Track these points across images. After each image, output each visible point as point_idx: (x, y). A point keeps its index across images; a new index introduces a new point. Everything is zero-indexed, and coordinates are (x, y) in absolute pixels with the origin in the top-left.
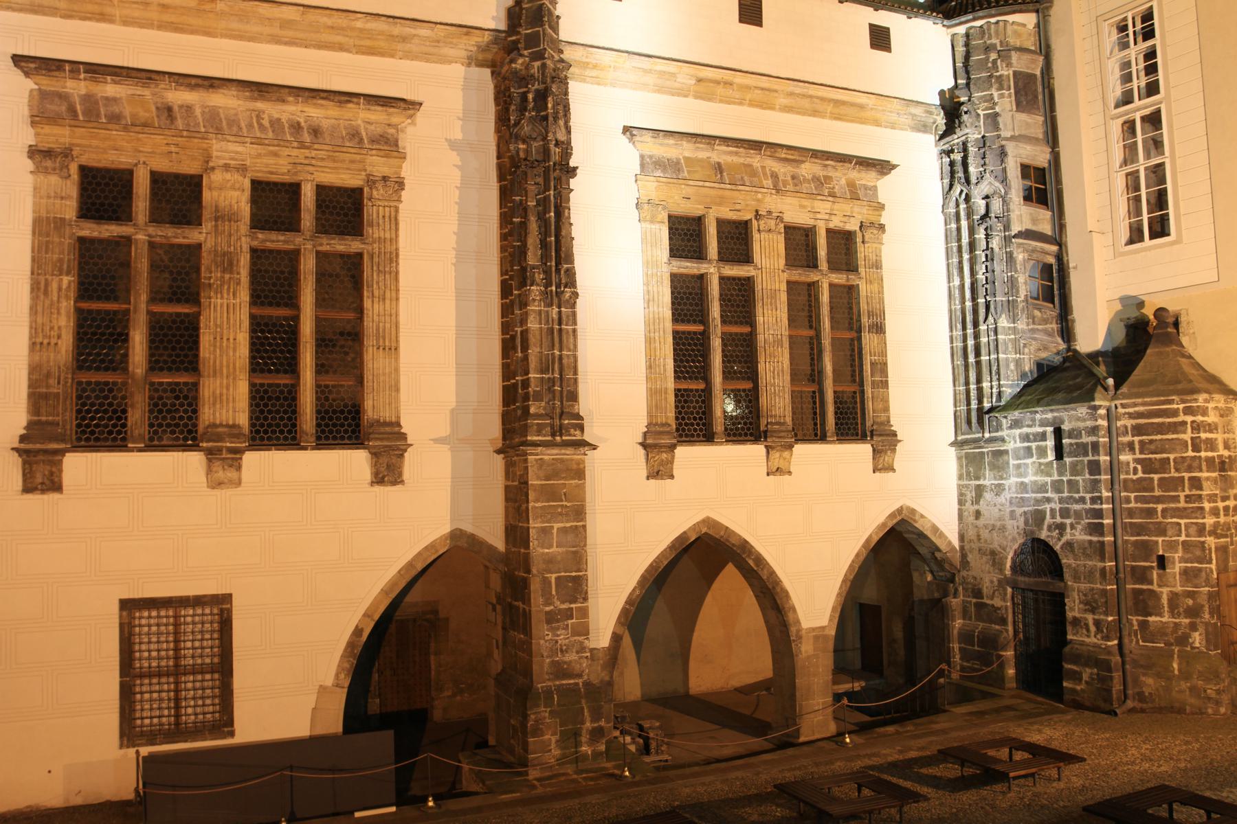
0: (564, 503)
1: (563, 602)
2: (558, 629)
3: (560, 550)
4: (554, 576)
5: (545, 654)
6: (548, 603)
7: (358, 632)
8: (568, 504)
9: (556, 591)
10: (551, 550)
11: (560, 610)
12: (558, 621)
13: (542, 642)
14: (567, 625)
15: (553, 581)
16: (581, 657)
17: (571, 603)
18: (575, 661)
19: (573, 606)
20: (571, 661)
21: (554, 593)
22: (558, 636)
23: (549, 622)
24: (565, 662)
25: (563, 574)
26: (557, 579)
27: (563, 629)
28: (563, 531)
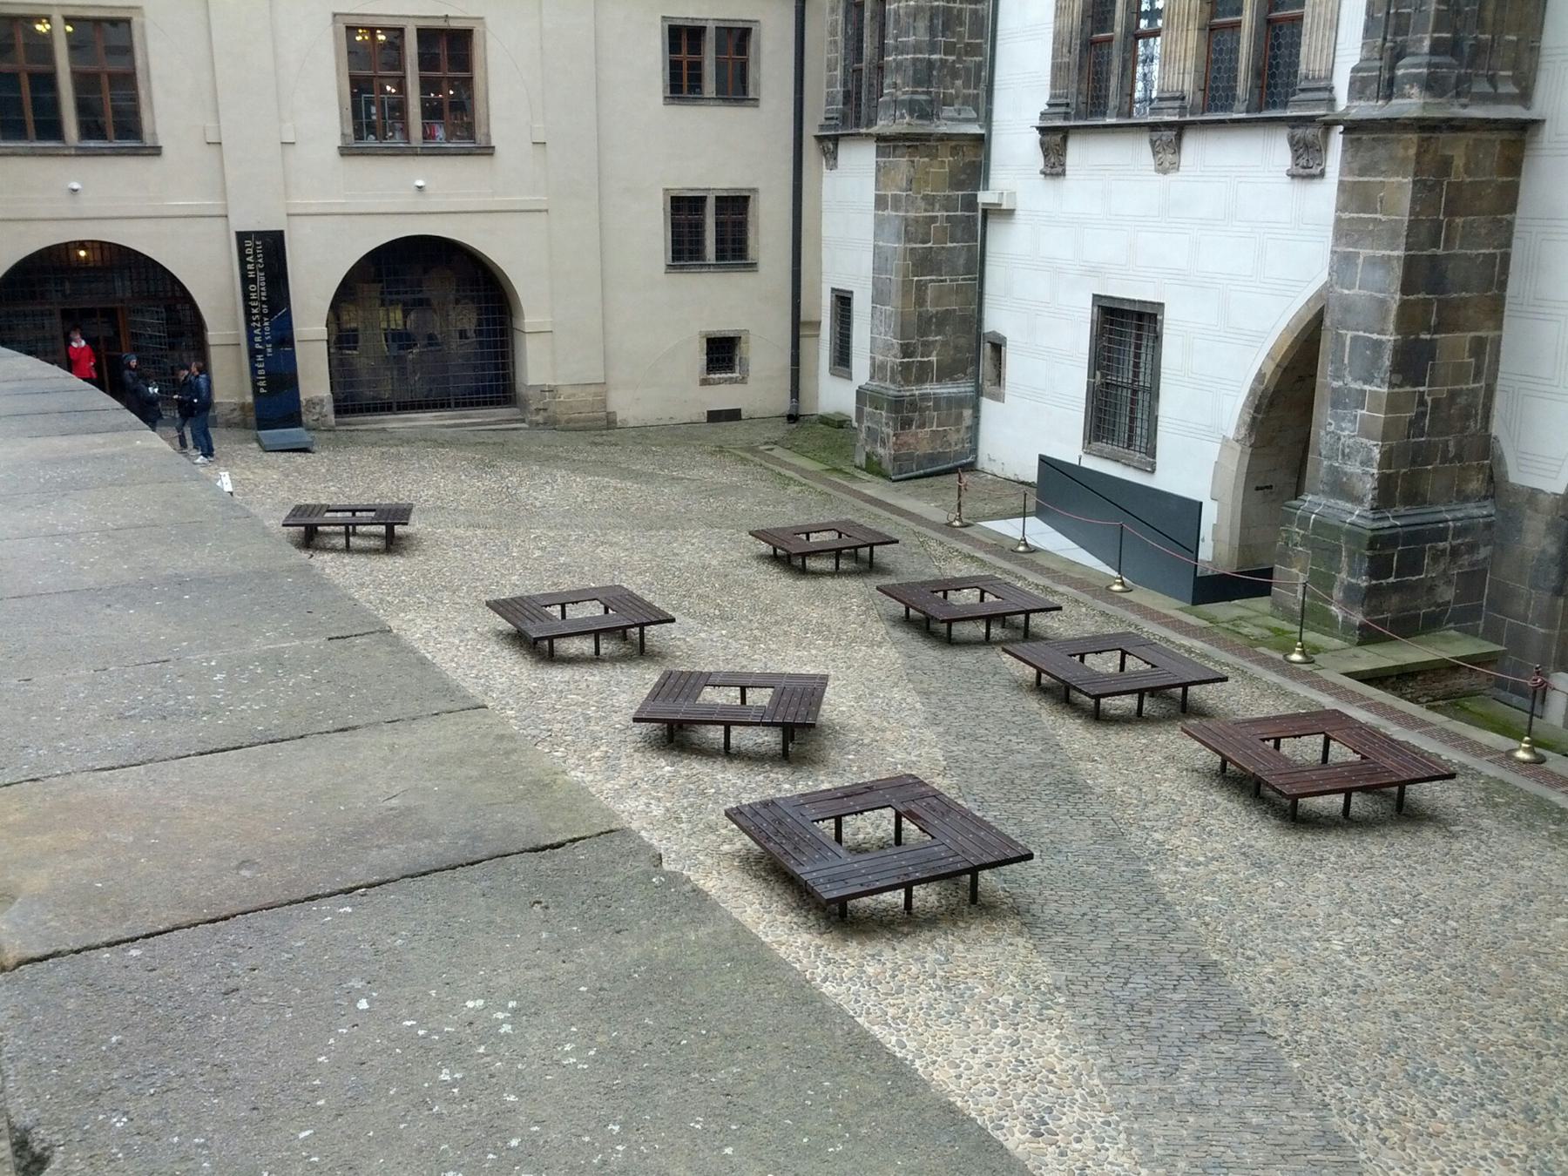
0: (1378, 216)
1: (1355, 380)
2: (1343, 419)
3: (1362, 292)
4: (1350, 334)
5: (1324, 453)
6: (1337, 377)
7: (1260, 376)
8: (1384, 218)
9: (1349, 358)
10: (1351, 292)
11: (1350, 390)
12: (1345, 407)
13: (1322, 433)
14: (1356, 416)
15: (1348, 342)
16: (1366, 473)
17: (1365, 382)
18: (1357, 475)
19: (1367, 387)
20: (1352, 474)
21: (1346, 361)
22: (1343, 430)
23: (1334, 405)
24: (1345, 474)
25: (1361, 333)
26: (1354, 339)
27: (1350, 421)
28: (1372, 262)
